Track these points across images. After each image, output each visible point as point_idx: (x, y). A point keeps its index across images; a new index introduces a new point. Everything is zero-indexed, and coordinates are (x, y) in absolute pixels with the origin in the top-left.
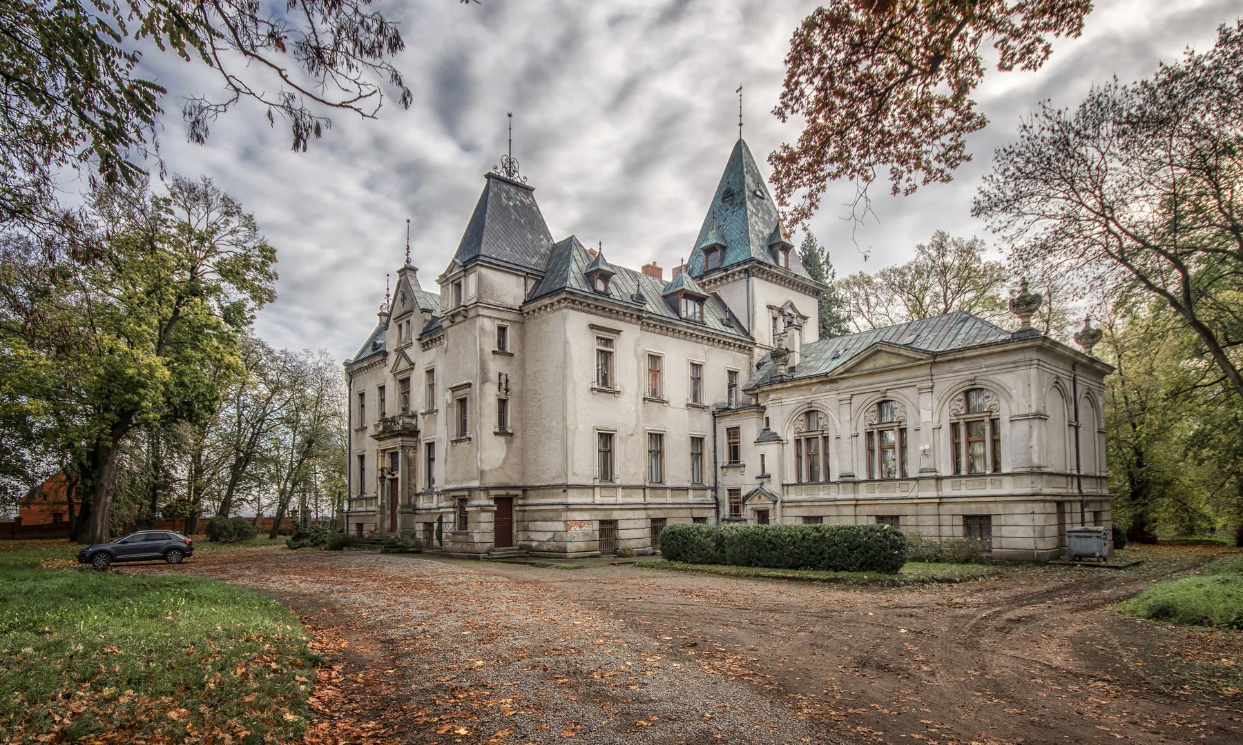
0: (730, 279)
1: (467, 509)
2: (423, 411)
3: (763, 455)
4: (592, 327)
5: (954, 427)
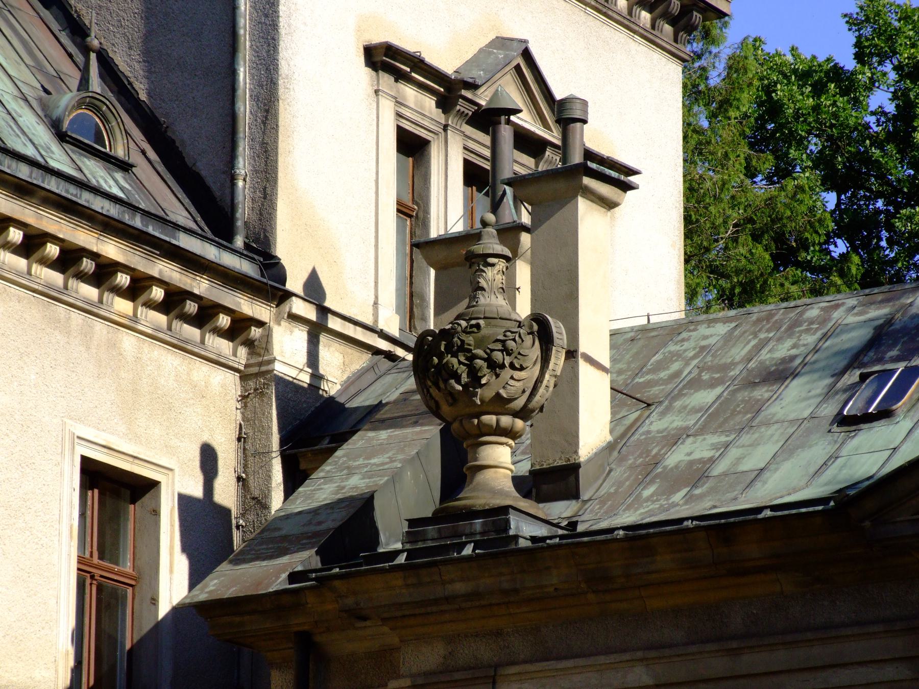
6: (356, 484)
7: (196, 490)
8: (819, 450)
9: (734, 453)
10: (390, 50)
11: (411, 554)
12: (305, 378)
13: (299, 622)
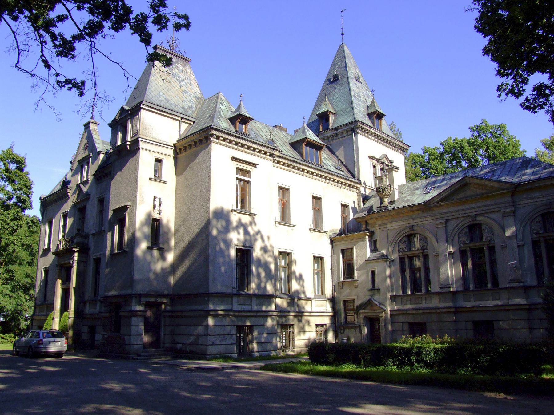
0: (340, 136)
1: (121, 314)
2: (94, 232)
3: (373, 272)
4: (233, 159)
5: (535, 244)
6: (371, 204)
7: (353, 206)
8: (422, 197)
9: (412, 198)
10: (371, 156)
11: (377, 211)
12: (364, 193)
13: (365, 220)
